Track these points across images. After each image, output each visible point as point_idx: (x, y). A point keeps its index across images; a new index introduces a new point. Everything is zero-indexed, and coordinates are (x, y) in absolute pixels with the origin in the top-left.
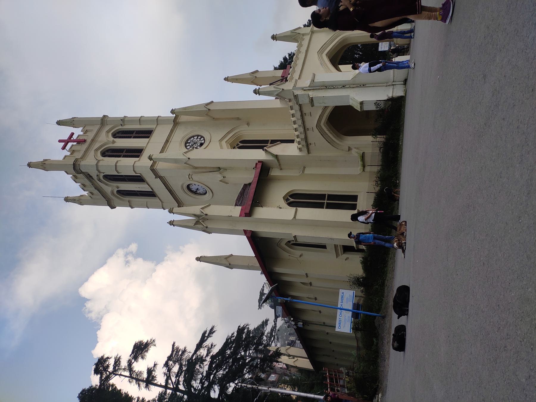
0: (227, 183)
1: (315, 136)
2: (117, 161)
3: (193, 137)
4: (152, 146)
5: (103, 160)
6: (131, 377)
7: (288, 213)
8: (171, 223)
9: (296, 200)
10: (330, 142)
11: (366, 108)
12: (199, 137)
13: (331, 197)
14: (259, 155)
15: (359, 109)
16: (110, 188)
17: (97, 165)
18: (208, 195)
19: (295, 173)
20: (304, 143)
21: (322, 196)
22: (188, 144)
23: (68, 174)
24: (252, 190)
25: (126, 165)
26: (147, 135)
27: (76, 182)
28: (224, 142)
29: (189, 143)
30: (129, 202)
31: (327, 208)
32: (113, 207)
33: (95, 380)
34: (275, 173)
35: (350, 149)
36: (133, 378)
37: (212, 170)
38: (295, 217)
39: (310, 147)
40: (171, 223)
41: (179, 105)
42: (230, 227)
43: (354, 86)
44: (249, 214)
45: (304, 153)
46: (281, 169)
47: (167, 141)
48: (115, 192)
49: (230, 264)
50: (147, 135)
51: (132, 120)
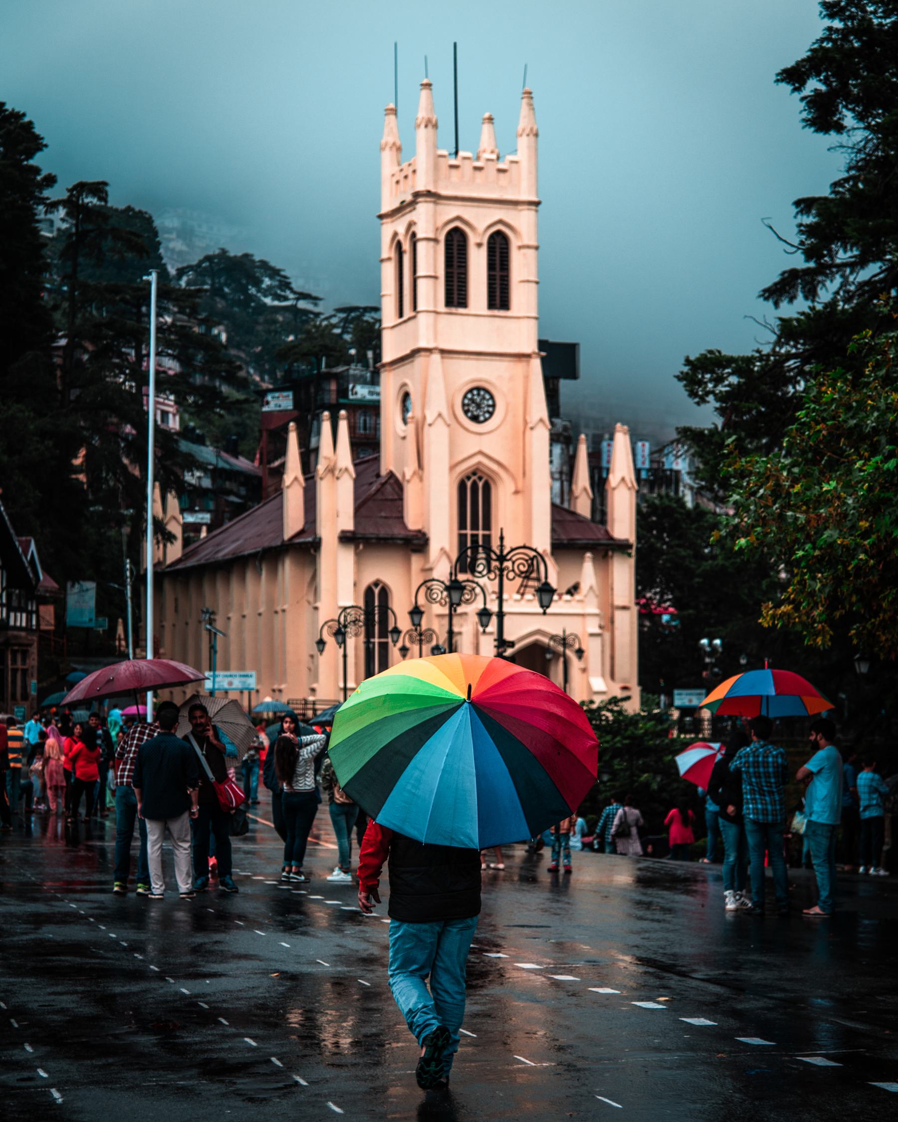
3: (492, 397)
12: (491, 409)
22: (475, 392)
28: (479, 458)
29: (479, 394)
34: (416, 561)
44: (346, 538)
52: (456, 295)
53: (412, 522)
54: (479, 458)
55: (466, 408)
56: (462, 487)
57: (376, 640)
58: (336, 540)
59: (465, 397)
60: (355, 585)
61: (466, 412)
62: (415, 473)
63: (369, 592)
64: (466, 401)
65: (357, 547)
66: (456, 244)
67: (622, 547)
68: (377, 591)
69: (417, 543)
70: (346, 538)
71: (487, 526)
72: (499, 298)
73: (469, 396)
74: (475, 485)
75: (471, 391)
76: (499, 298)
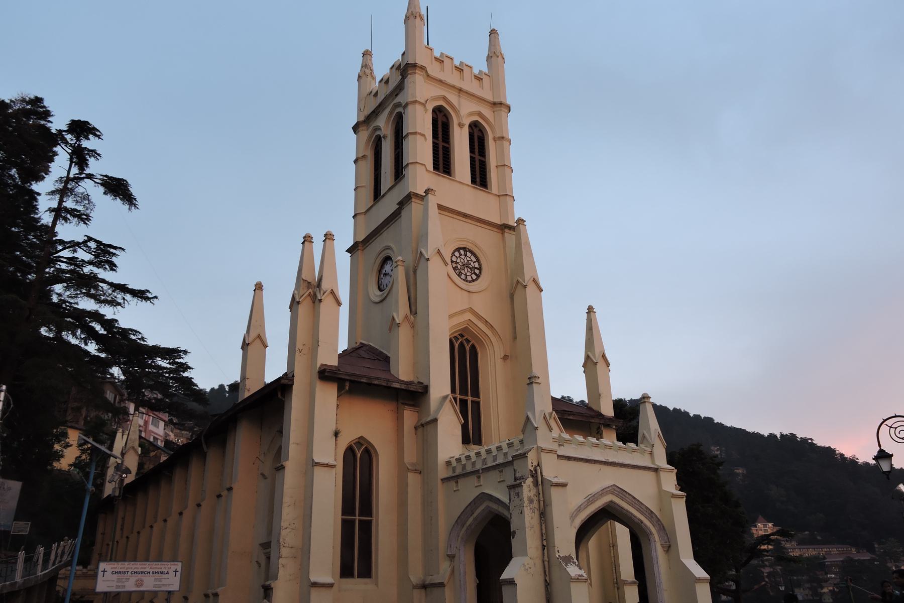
0: (390, 330)
1: (469, 491)
2: (423, 135)
3: (478, 260)
4: (457, 190)
5: (426, 110)
6: (68, 179)
7: (329, 452)
8: (307, 239)
9: (359, 462)
10: (460, 521)
11: (506, 591)
12: (477, 271)
13: (367, 528)
14: (440, 384)
15: (505, 576)
16: (384, 124)
17: (415, 102)
18: (375, 294)
19: (410, 456)
20: (459, 471)
21: (367, 507)
22: (462, 252)
23: (403, 54)
24: (376, 375)
25: (420, 149)
26: (478, 180)
27: (392, 68)
30: (364, 157)
31: (344, 522)
32: (356, 128)
33: (58, 123)
34: (409, 417)
35: (451, 557)
36: (67, 182)
37: (412, 300)
38: (318, 464)
39: (453, 483)
40: (307, 239)
41: (533, 233)
42: (299, 345)
43: (546, 563)
45: (442, 473)
46: (416, 428)
47: (465, 216)
48: (378, 133)
49: (248, 344)
50: (478, 180)
51: (503, 154)
52: (443, 163)
54: (468, 316)
55: (454, 265)
58: (316, 375)
59: (453, 254)
60: (336, 434)
61: (454, 268)
62: (406, 317)
63: (350, 450)
64: (454, 259)
65: (340, 389)
69: (414, 395)
70: (326, 375)
71: (476, 393)
73: (457, 254)
74: (461, 345)
75: (458, 250)
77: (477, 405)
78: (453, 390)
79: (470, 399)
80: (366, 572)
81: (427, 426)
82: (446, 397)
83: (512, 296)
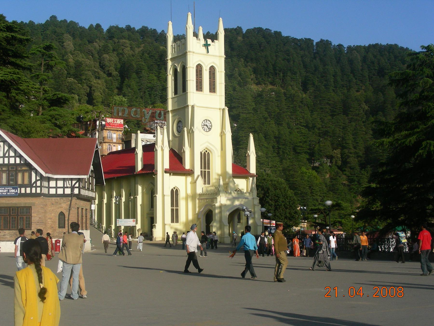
3: (211, 123)
9: (175, 193)
12: (210, 127)
13: (177, 210)
15: (210, 225)
19: (189, 192)
21: (177, 205)
44: (166, 171)
52: (199, 87)
53: (187, 166)
56: (201, 153)
57: (175, 208)
63: (172, 191)
65: (170, 175)
66: (199, 69)
67: (252, 176)
68: (175, 190)
72: (213, 89)
73: (204, 122)
74: (205, 153)
75: (204, 121)
76: (213, 89)
77: (209, 172)
78: (201, 168)
79: (207, 170)
80: (177, 221)
81: (194, 183)
82: (198, 176)
83: (222, 136)
